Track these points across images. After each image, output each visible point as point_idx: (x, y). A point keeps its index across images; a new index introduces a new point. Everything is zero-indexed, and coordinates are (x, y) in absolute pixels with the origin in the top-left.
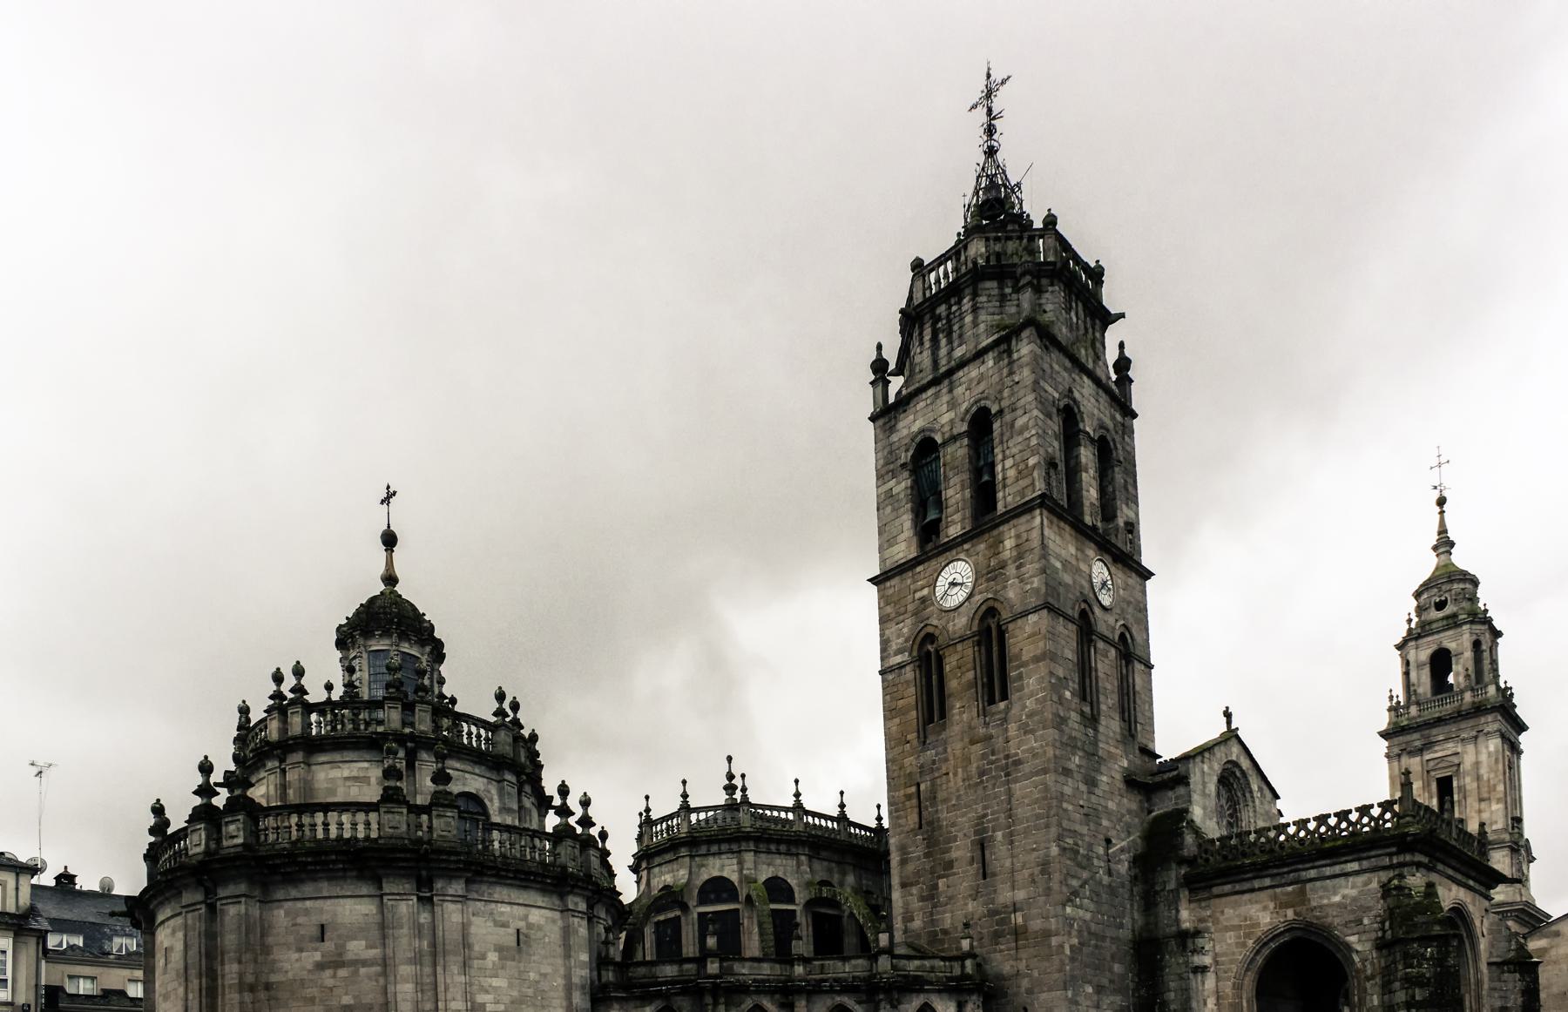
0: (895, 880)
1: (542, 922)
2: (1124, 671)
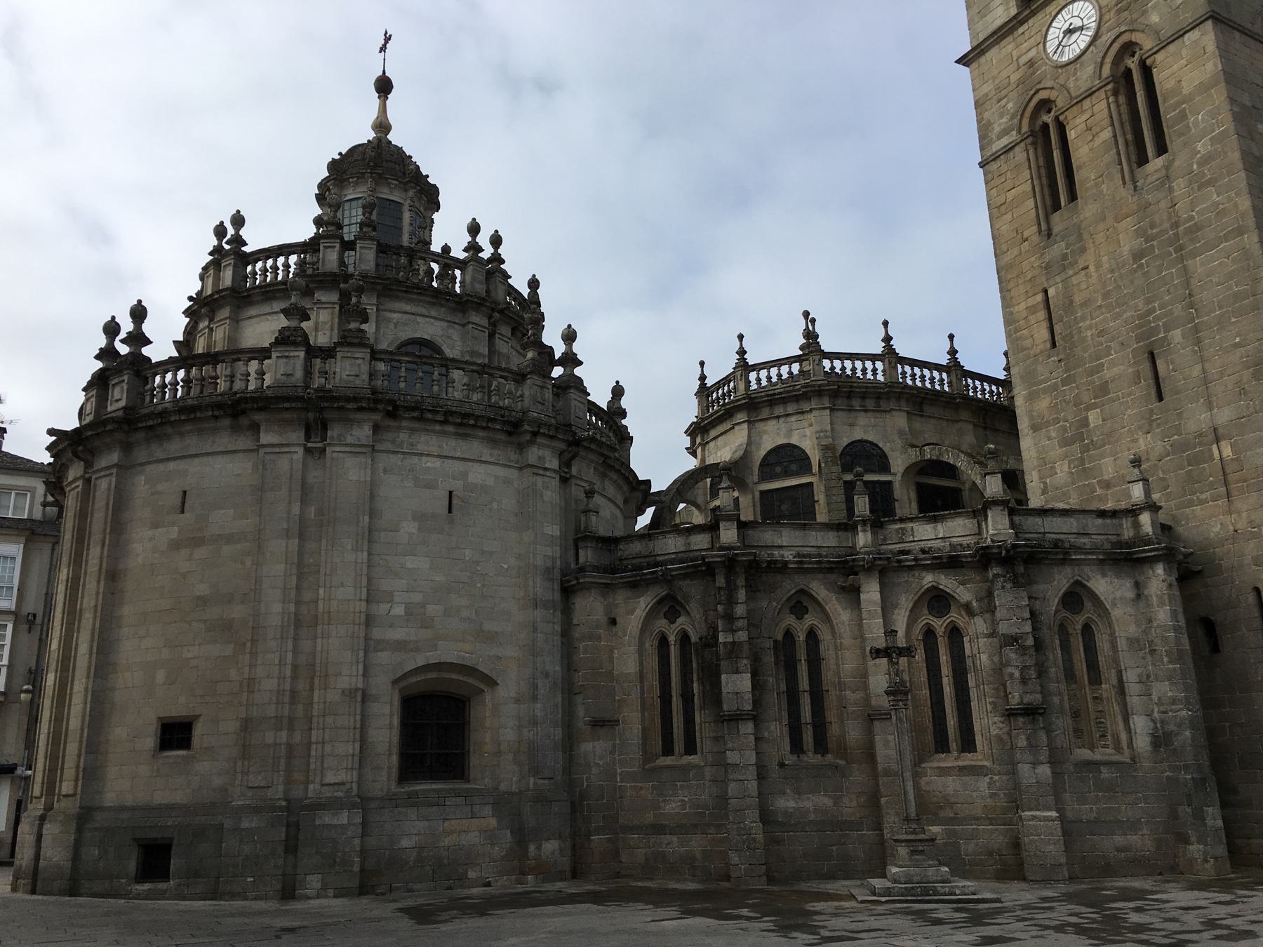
0: (1023, 424)
1: (490, 482)
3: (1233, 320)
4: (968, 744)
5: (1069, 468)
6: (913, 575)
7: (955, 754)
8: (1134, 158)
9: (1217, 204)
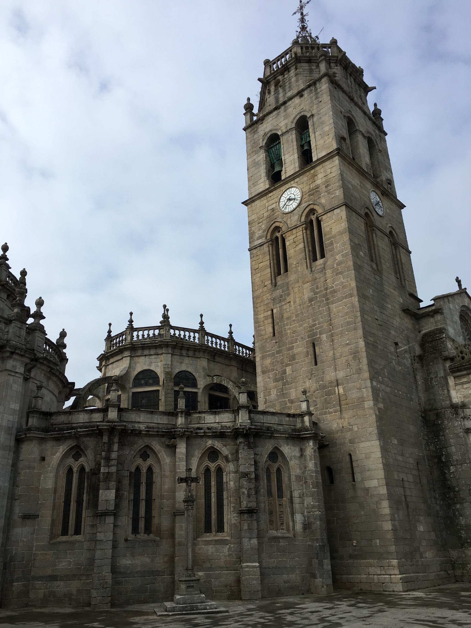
0: (259, 370)
2: (394, 253)
3: (346, 333)
4: (220, 529)
5: (277, 392)
6: (203, 440)
7: (214, 533)
8: (312, 258)
9: (343, 283)
